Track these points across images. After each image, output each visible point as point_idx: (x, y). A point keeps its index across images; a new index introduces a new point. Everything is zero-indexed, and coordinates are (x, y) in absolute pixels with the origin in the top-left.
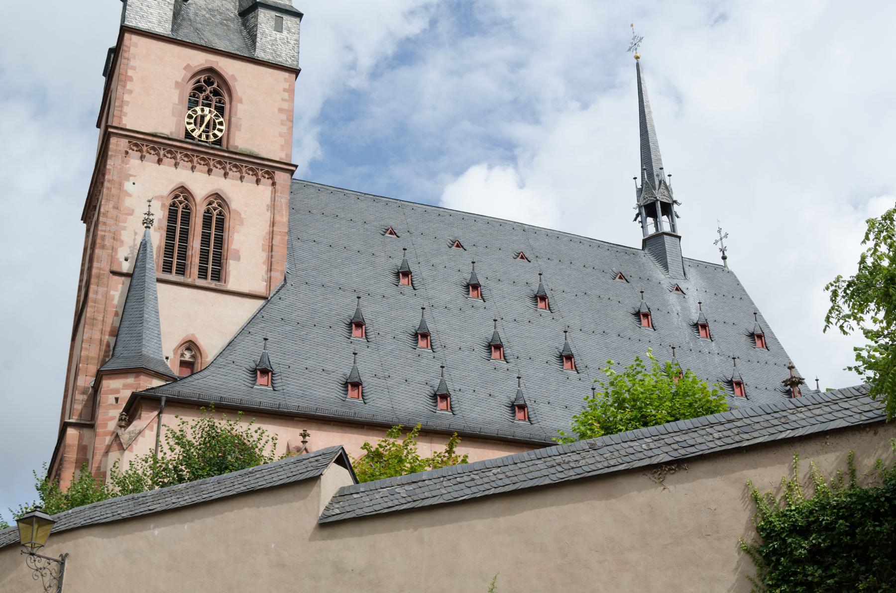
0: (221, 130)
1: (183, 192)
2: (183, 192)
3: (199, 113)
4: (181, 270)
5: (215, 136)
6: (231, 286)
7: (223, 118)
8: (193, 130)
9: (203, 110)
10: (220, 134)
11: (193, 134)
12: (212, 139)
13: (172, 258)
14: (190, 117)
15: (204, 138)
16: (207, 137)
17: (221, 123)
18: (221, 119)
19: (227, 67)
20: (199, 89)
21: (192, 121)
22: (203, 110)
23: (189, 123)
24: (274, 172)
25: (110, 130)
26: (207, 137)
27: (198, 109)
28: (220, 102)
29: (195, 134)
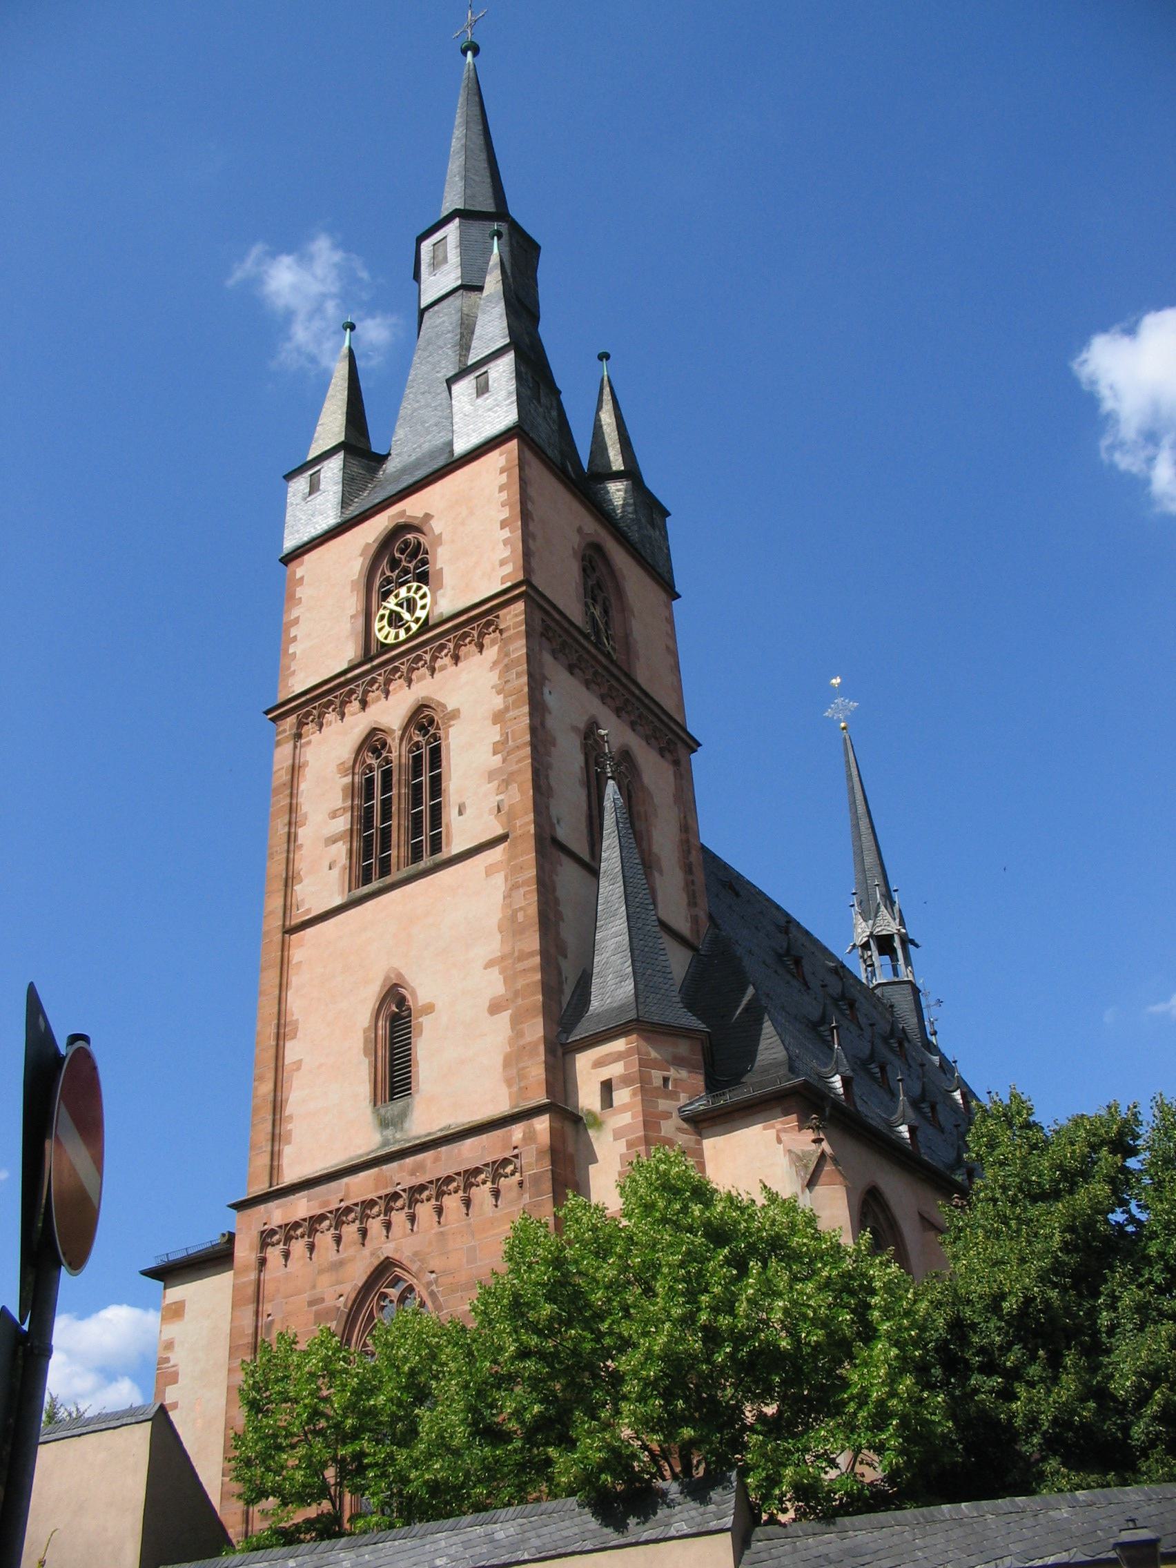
1: (374, 742)
4: (385, 869)
7: (427, 584)
12: (415, 627)
24: (497, 617)
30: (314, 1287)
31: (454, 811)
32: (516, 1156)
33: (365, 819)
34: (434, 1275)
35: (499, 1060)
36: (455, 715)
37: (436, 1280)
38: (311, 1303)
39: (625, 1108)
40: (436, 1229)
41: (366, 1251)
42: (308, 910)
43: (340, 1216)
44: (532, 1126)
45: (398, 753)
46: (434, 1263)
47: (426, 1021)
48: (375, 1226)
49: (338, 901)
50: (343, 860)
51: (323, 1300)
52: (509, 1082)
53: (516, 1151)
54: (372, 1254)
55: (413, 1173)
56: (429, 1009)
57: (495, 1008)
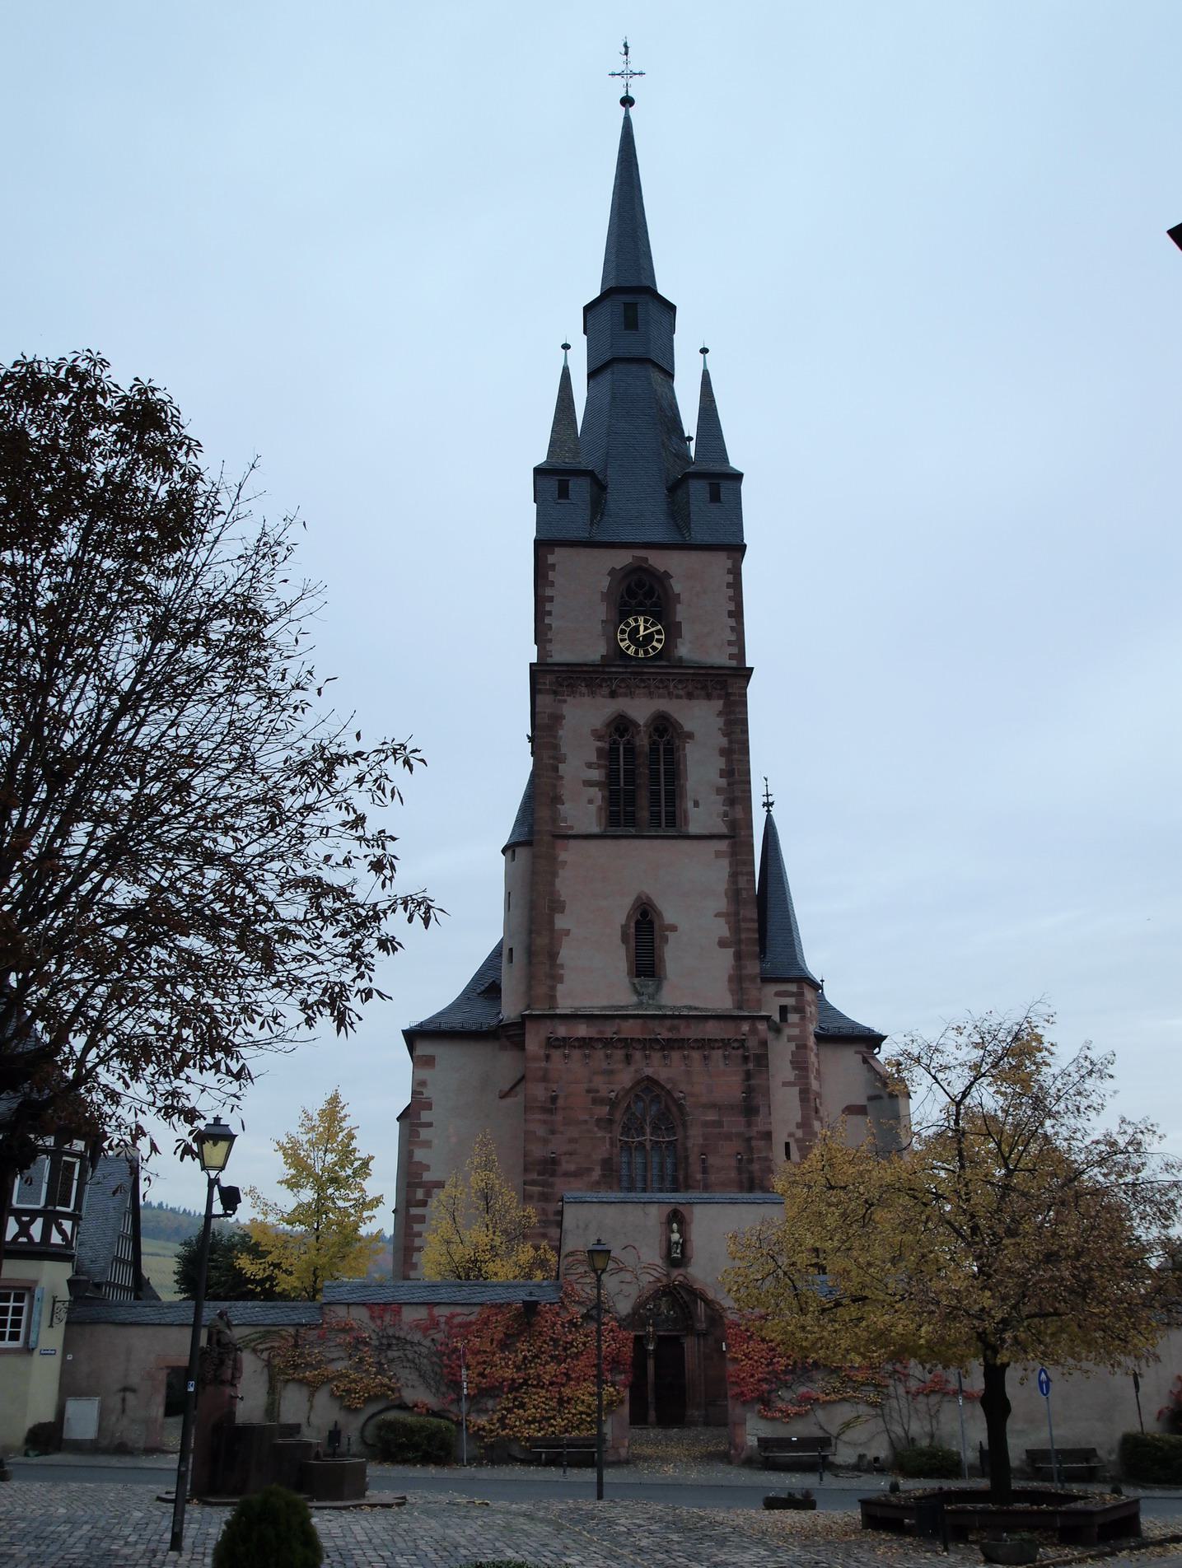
0: (659, 641)
1: (621, 725)
2: (621, 725)
3: (633, 624)
5: (654, 648)
6: (693, 829)
8: (628, 648)
9: (636, 621)
10: (660, 646)
11: (629, 652)
12: (652, 653)
13: (619, 806)
14: (623, 632)
15: (641, 654)
16: (646, 652)
17: (659, 632)
18: (660, 627)
19: (659, 561)
20: (630, 593)
21: (626, 636)
22: (636, 621)
23: (622, 640)
25: (533, 668)
26: (646, 652)
27: (631, 620)
28: (655, 605)
29: (631, 651)
30: (590, 1081)
31: (690, 804)
32: (744, 1040)
33: (612, 777)
34: (682, 1095)
35: (726, 978)
36: (690, 736)
37: (684, 1098)
38: (589, 1091)
39: (794, 1025)
40: (683, 1068)
41: (632, 1069)
42: (571, 828)
43: (608, 1043)
44: (754, 1025)
45: (643, 741)
46: (683, 1087)
47: (671, 935)
48: (638, 1055)
49: (595, 829)
50: (599, 802)
51: (598, 1091)
52: (732, 992)
53: (744, 1037)
54: (636, 1071)
55: (670, 1030)
56: (674, 928)
57: (722, 944)
